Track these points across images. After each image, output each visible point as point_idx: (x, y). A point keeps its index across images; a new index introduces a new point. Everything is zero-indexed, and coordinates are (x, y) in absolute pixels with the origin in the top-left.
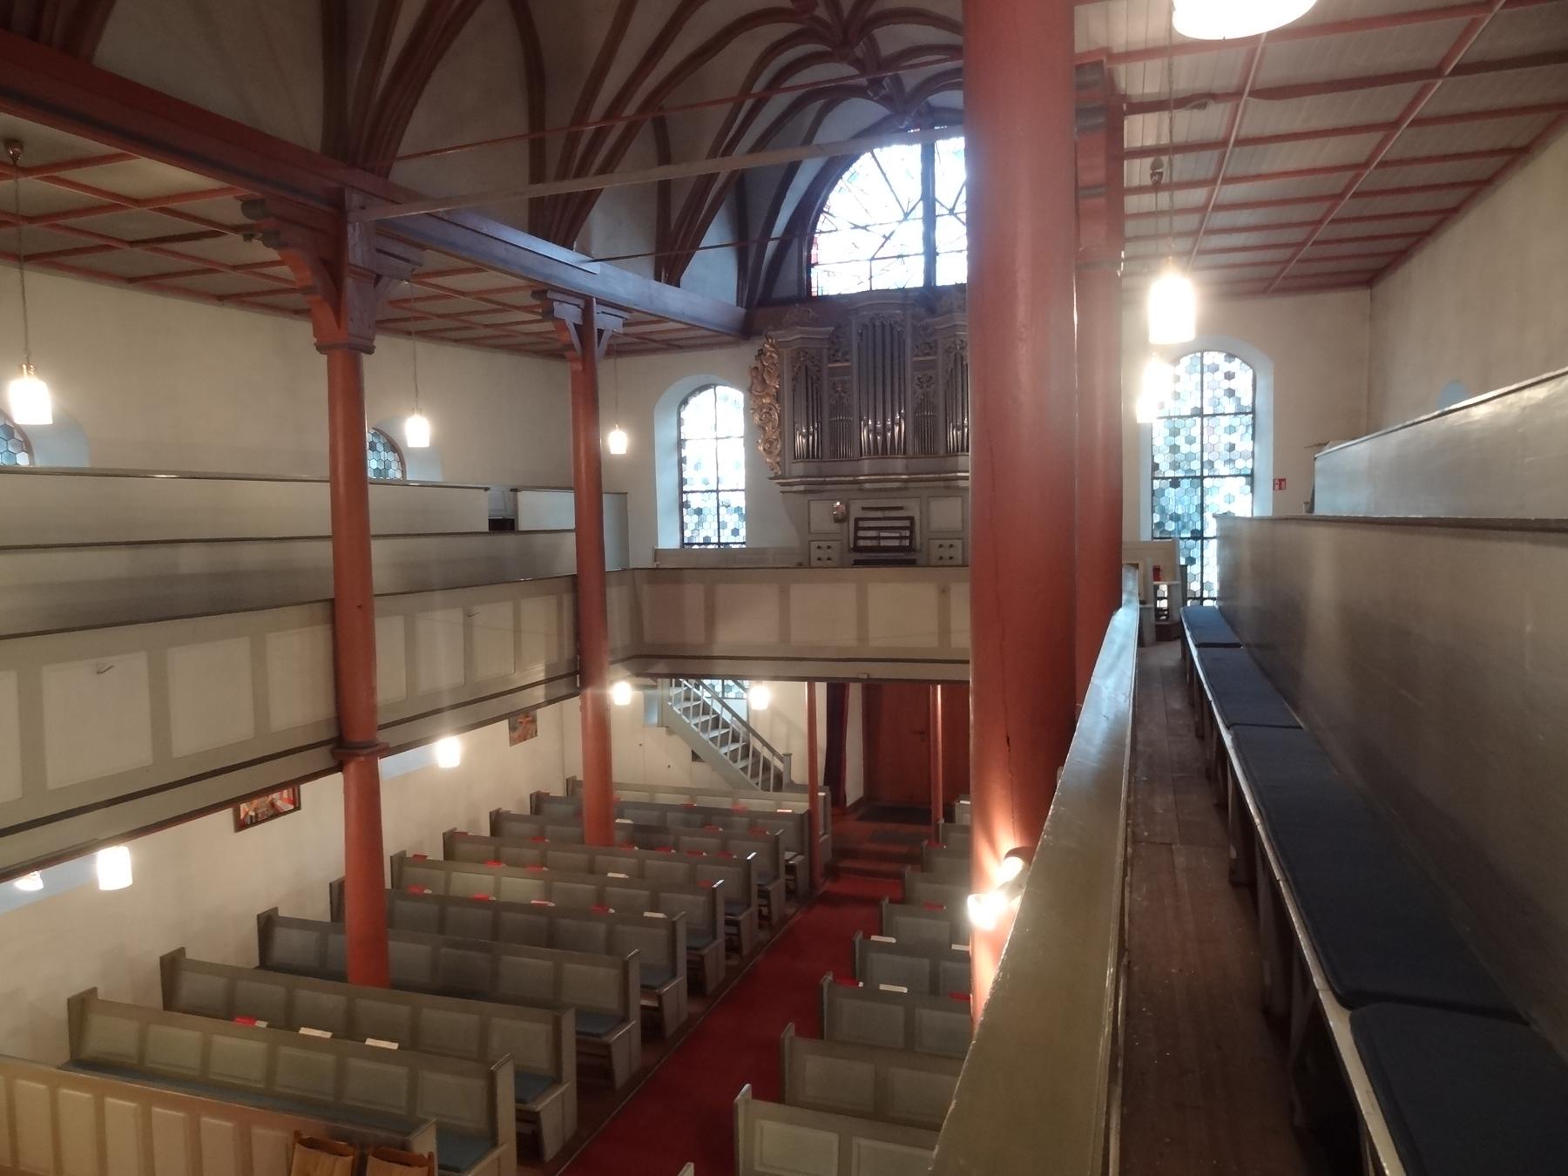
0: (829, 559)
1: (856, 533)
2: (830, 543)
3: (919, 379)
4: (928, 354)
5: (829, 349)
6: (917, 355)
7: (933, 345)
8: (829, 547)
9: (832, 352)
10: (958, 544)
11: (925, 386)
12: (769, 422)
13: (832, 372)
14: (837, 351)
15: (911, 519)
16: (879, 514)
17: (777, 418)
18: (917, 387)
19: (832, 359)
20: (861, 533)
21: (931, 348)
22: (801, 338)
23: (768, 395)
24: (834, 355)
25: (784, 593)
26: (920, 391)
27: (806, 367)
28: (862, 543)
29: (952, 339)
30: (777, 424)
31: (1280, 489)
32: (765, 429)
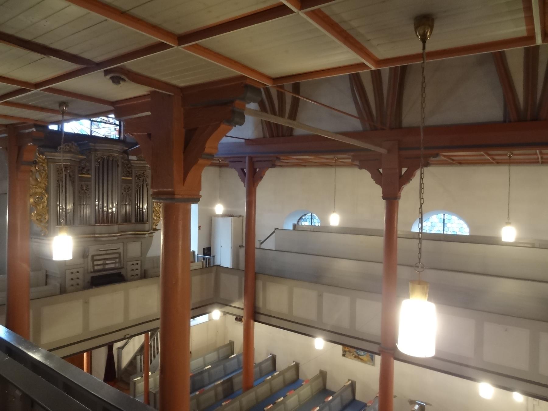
0: (78, 278)
1: (93, 263)
2: (78, 270)
3: (124, 187)
4: (128, 176)
5: (79, 167)
6: (123, 176)
7: (130, 172)
8: (78, 272)
9: (81, 169)
10: (139, 262)
11: (127, 190)
12: (40, 203)
13: (81, 179)
14: (83, 168)
15: (119, 253)
16: (104, 252)
17: (46, 202)
18: (123, 191)
19: (81, 172)
20: (96, 263)
21: (129, 173)
22: (70, 160)
23: (40, 187)
24: (82, 170)
25: (86, 303)
26: (125, 193)
27: (70, 175)
28: (96, 268)
29: (142, 172)
30: (46, 204)
31: (200, 229)
32: (37, 207)
